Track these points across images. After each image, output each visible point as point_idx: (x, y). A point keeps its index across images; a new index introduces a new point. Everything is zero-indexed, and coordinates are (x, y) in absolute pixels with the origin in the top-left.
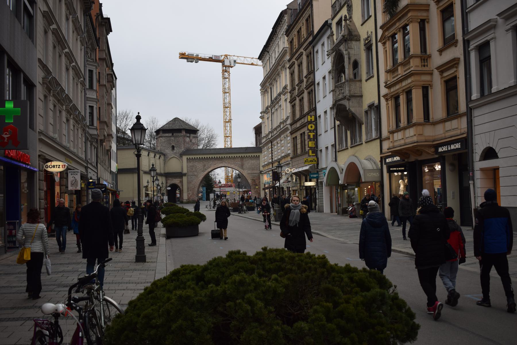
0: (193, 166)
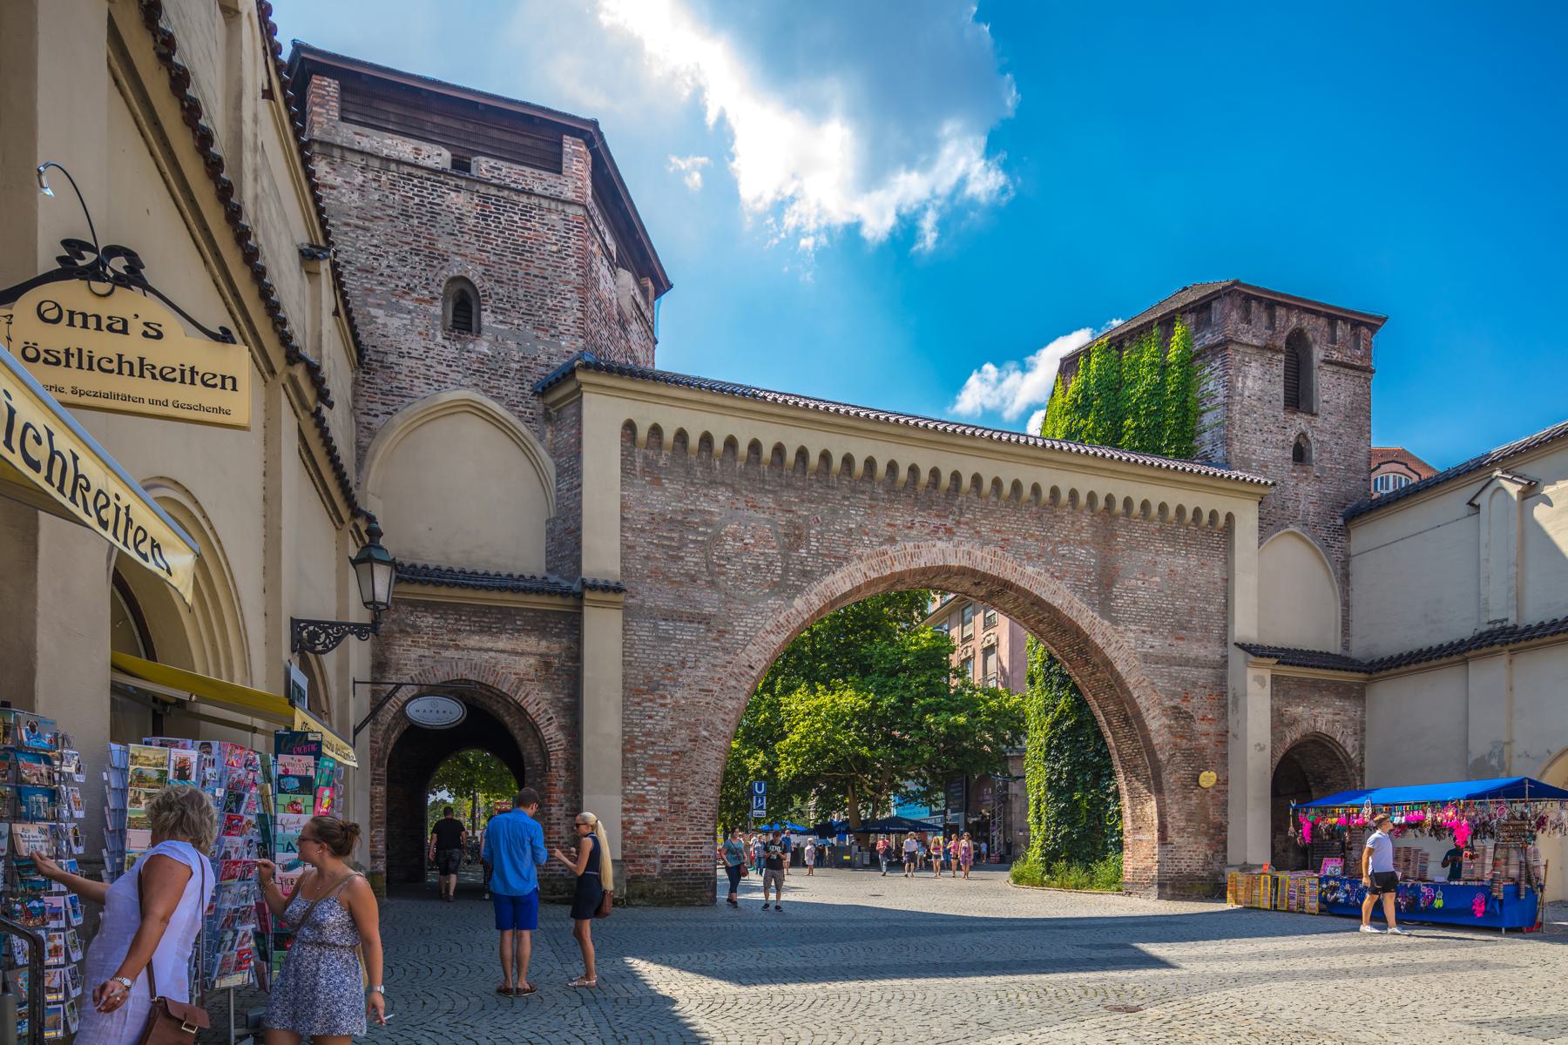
0: (681, 523)
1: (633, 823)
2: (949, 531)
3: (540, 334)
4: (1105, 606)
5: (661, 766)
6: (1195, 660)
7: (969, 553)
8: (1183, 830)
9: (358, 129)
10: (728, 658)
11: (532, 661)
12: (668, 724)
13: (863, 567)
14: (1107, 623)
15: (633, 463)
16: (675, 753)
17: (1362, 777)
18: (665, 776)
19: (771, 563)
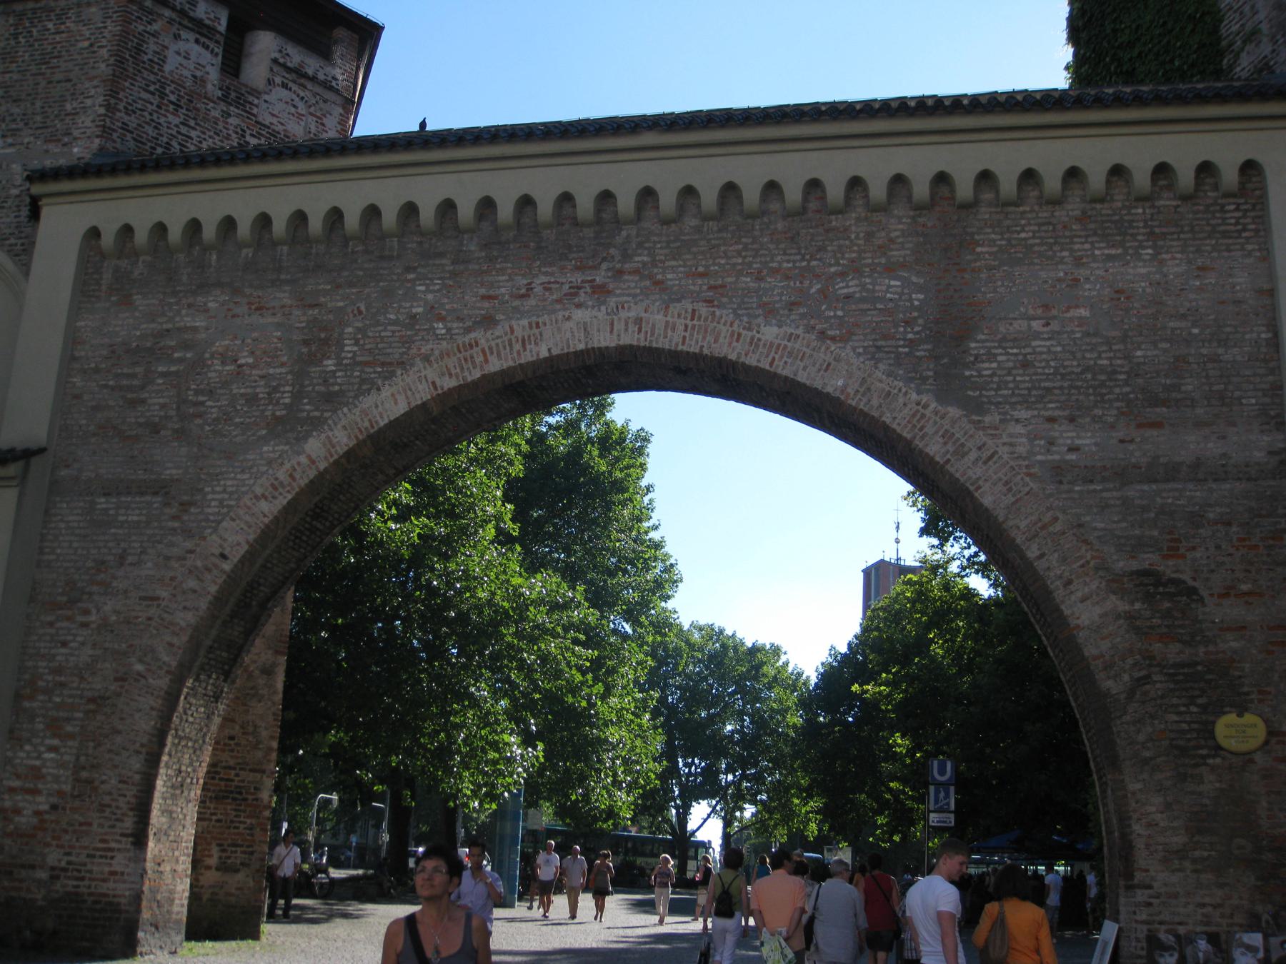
1: (17, 811)
2: (601, 292)
5: (68, 720)
6: (1197, 464)
7: (639, 321)
10: (189, 545)
13: (431, 373)
14: (954, 412)
16: (92, 700)
18: (71, 736)
19: (276, 389)
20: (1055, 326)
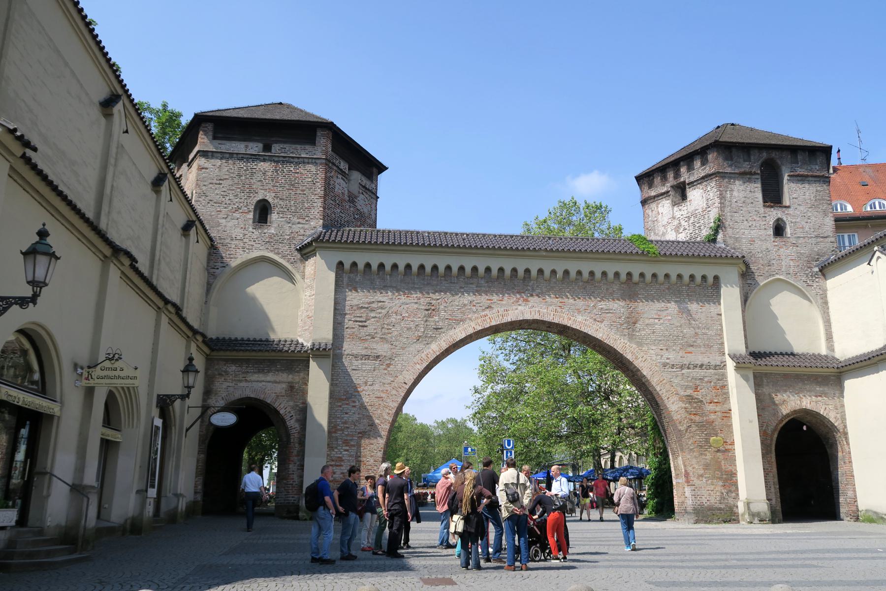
3: (300, 220)
4: (631, 337)
8: (702, 476)
9: (220, 142)
11: (284, 386)
12: (356, 417)
13: (473, 324)
15: (342, 281)
17: (847, 439)
18: (354, 446)
20: (661, 321)
